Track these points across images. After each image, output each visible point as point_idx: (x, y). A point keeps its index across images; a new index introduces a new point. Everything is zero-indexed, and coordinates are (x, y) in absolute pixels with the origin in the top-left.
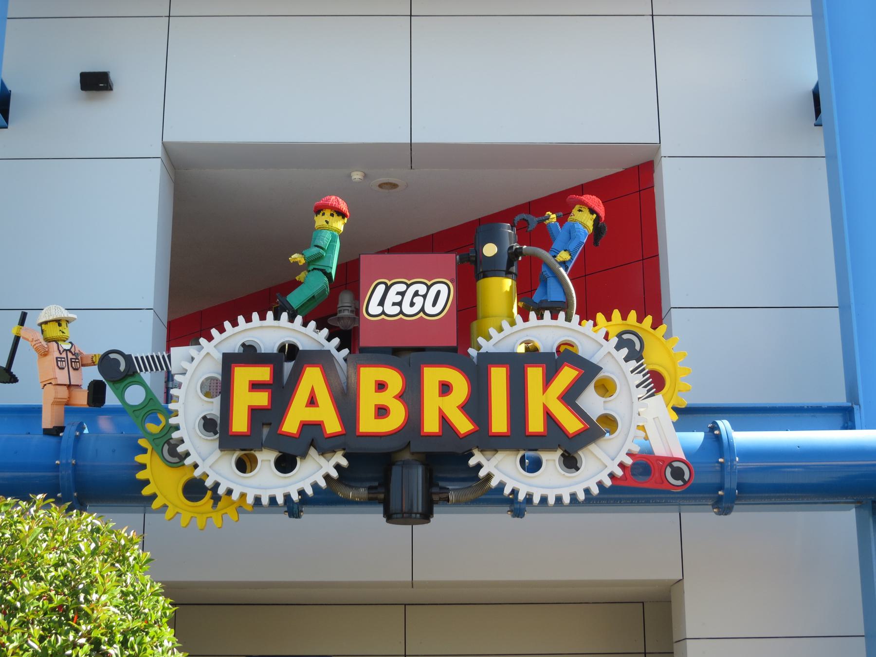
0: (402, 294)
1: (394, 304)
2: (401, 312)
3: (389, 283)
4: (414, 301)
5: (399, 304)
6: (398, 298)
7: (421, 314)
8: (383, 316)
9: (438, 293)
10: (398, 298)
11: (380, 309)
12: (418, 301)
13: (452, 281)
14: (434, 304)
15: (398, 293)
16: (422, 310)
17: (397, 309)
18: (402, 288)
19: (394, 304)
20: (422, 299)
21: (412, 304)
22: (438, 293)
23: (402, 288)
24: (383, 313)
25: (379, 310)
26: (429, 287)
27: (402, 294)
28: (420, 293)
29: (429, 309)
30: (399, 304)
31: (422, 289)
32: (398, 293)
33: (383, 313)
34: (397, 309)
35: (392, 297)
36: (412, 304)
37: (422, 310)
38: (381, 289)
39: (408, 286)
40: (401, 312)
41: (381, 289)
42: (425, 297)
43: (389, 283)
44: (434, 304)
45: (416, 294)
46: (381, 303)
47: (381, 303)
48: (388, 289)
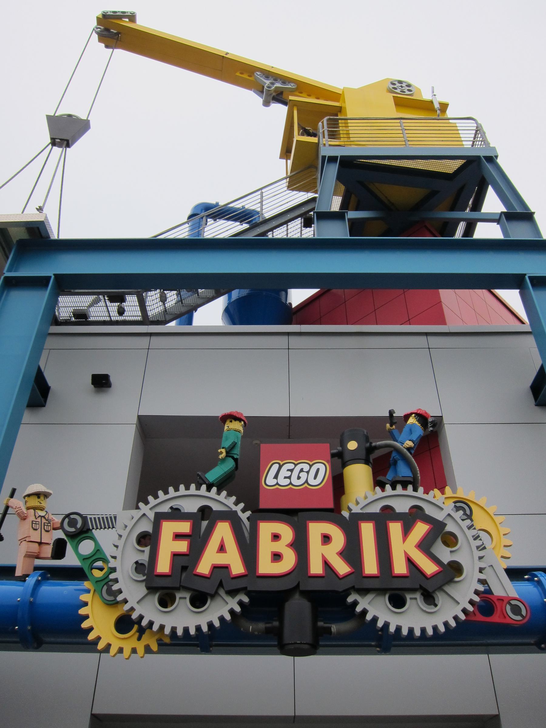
0: (291, 471)
1: (285, 478)
2: (291, 483)
3: (282, 463)
4: (300, 475)
5: (289, 477)
6: (289, 474)
7: (306, 485)
8: (277, 486)
9: (318, 470)
10: (289, 474)
11: (275, 481)
12: (303, 475)
13: (327, 462)
14: (315, 478)
15: (288, 470)
16: (306, 482)
17: (287, 481)
18: (291, 466)
19: (285, 478)
20: (306, 474)
21: (299, 478)
22: (318, 470)
23: (291, 466)
24: (277, 484)
25: (275, 481)
26: (311, 466)
27: (291, 471)
28: (304, 470)
29: (312, 481)
31: (306, 467)
32: (288, 470)
33: (277, 484)
34: (287, 481)
35: (284, 472)
36: (299, 478)
37: (306, 482)
38: (276, 466)
39: (296, 465)
41: (275, 467)
42: (308, 472)
43: (282, 463)
44: (315, 478)
45: (302, 470)
46: (276, 477)
47: (276, 477)
48: (280, 467)
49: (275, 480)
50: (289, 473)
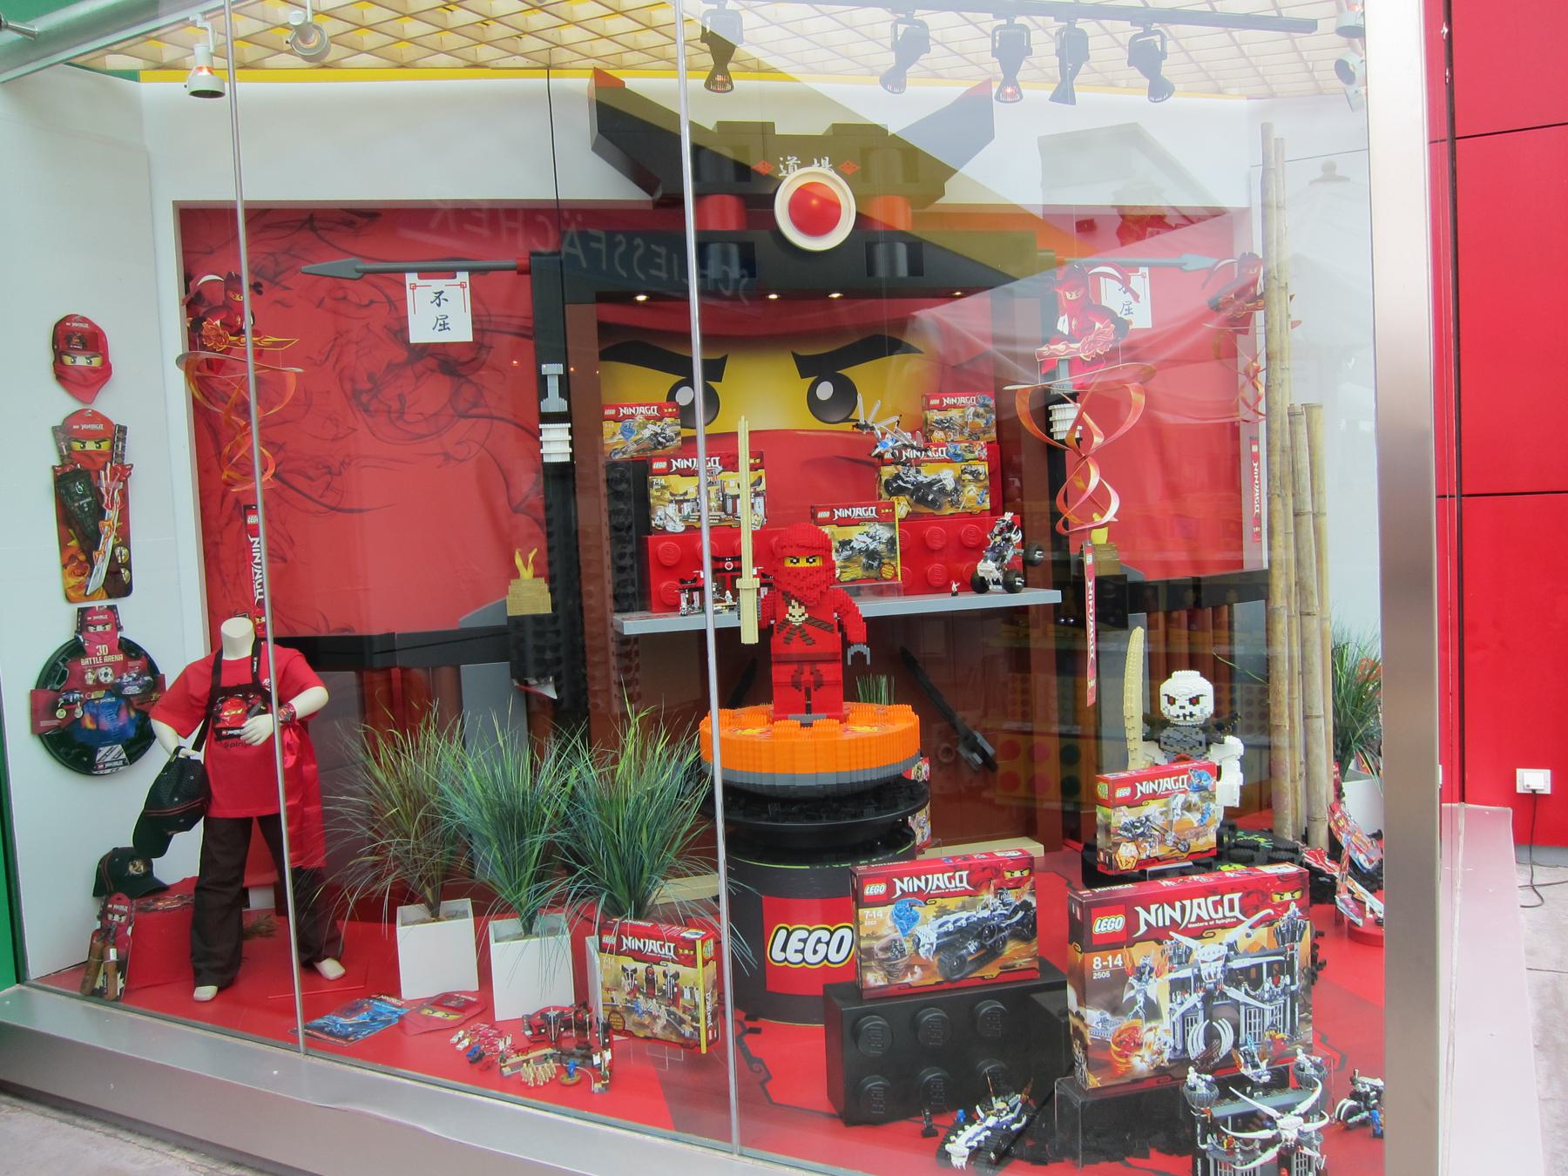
0: (804, 941)
1: (796, 951)
2: (804, 960)
3: (790, 929)
5: (802, 951)
6: (801, 945)
9: (842, 939)
10: (801, 945)
12: (822, 948)
14: (838, 951)
15: (800, 940)
16: (826, 957)
17: (799, 957)
18: (804, 934)
19: (796, 951)
21: (815, 952)
22: (842, 939)
23: (804, 934)
24: (786, 959)
26: (832, 934)
27: (804, 941)
29: (834, 957)
30: (802, 951)
31: (825, 936)
32: (800, 940)
33: (786, 959)
34: (799, 957)
35: (794, 943)
36: (815, 952)
37: (826, 957)
38: (783, 933)
39: (810, 933)
40: (804, 960)
41: (782, 934)
42: (828, 943)
44: (838, 951)
45: (819, 941)
46: (784, 949)
47: (784, 949)
48: (789, 934)
49: (783, 954)
50: (802, 944)
